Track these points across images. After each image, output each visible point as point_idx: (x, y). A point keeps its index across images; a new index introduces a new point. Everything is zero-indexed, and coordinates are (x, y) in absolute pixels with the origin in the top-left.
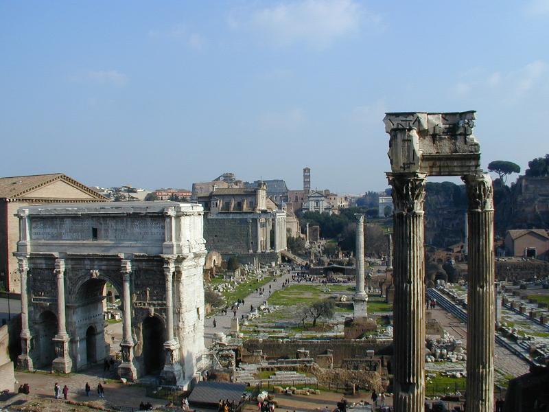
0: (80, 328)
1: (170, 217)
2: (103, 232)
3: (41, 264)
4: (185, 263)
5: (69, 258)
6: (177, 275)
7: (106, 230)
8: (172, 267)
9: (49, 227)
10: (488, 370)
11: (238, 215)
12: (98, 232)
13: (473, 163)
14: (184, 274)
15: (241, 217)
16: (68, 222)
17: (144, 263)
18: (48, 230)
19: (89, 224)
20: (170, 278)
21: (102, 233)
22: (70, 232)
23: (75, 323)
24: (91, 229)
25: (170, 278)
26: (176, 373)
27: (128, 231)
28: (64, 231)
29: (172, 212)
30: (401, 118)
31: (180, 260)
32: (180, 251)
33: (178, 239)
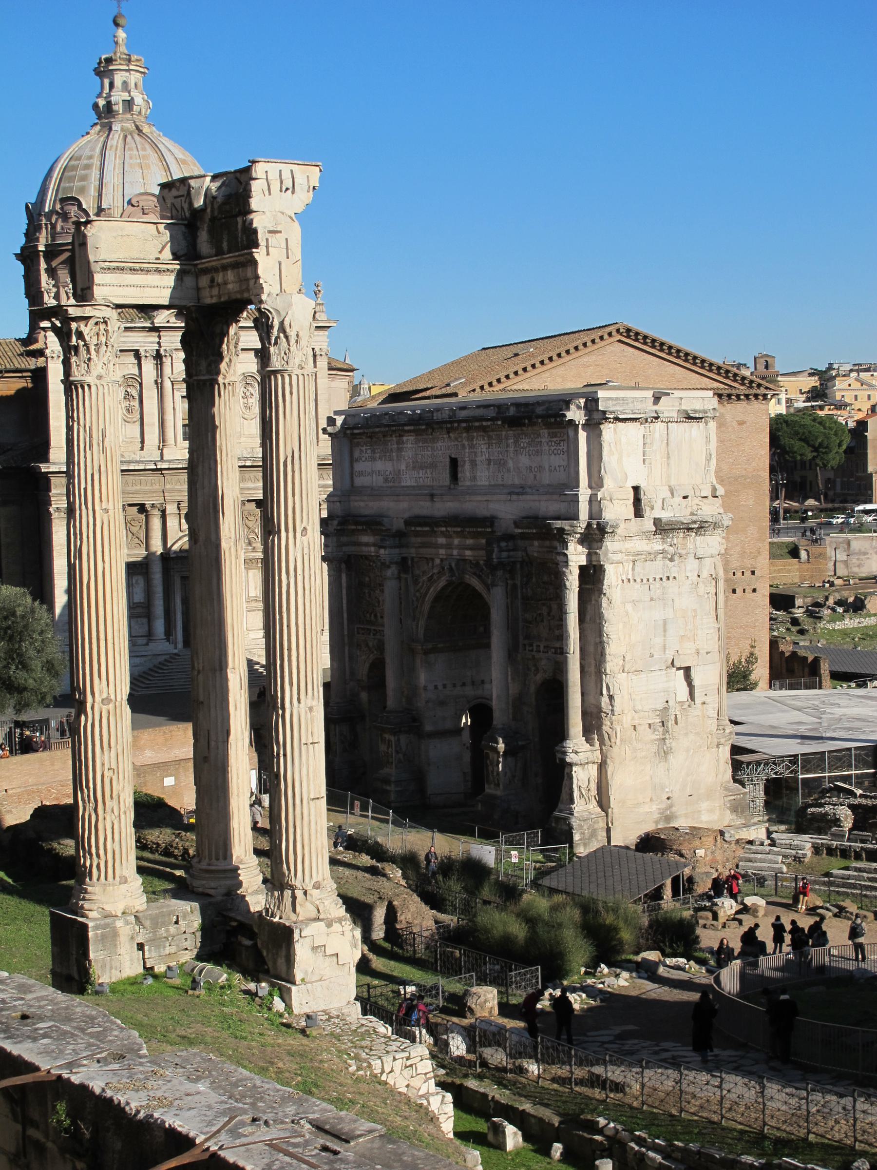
0: (442, 703)
2: (467, 466)
3: (367, 545)
4: (610, 545)
6: (592, 576)
7: (473, 463)
8: (576, 555)
9: (380, 458)
10: (280, 712)
12: (459, 469)
13: (249, 273)
14: (612, 577)
17: (536, 543)
18: (379, 465)
19: (443, 447)
21: (465, 472)
22: (414, 468)
23: (425, 688)
24: (448, 460)
27: (511, 464)
28: (403, 467)
30: (174, 192)
31: (595, 535)
32: (596, 512)
33: (596, 482)
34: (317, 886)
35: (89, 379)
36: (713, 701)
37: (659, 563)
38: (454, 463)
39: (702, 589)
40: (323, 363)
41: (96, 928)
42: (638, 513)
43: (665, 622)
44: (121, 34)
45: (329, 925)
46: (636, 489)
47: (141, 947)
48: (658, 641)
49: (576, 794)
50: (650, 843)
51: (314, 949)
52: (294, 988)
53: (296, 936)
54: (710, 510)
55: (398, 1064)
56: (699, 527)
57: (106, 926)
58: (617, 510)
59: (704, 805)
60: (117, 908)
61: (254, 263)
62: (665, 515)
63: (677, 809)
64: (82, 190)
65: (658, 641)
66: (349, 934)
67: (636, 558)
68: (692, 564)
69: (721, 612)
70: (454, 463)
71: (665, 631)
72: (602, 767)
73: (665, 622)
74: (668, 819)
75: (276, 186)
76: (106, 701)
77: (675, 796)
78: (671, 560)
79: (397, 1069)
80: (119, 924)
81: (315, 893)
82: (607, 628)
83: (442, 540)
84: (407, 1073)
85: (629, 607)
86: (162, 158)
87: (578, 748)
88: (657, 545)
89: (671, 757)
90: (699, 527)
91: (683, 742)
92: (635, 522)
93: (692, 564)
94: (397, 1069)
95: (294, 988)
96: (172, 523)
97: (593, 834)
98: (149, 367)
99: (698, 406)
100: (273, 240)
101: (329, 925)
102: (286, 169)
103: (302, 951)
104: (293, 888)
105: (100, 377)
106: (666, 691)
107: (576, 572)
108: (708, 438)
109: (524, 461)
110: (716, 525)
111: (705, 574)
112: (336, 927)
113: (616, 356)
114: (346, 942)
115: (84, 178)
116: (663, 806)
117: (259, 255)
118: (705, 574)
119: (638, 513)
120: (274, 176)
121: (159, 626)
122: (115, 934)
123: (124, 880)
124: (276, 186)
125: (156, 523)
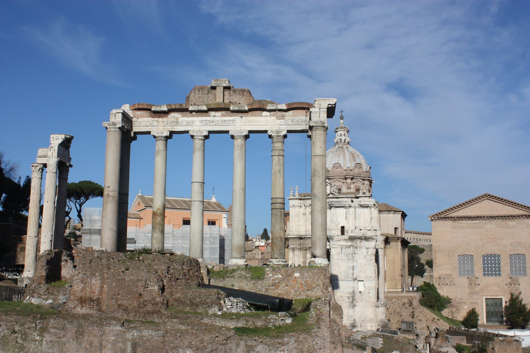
39: (368, 257)
43: (353, 267)
44: (342, 121)
56: (367, 239)
63: (358, 324)
68: (364, 250)
71: (353, 269)
73: (353, 267)
77: (357, 320)
78: (356, 248)
85: (340, 261)
88: (349, 243)
89: (355, 308)
90: (367, 239)
102: (57, 135)
116: (352, 322)
119: (343, 233)
120: (55, 137)
124: (55, 139)
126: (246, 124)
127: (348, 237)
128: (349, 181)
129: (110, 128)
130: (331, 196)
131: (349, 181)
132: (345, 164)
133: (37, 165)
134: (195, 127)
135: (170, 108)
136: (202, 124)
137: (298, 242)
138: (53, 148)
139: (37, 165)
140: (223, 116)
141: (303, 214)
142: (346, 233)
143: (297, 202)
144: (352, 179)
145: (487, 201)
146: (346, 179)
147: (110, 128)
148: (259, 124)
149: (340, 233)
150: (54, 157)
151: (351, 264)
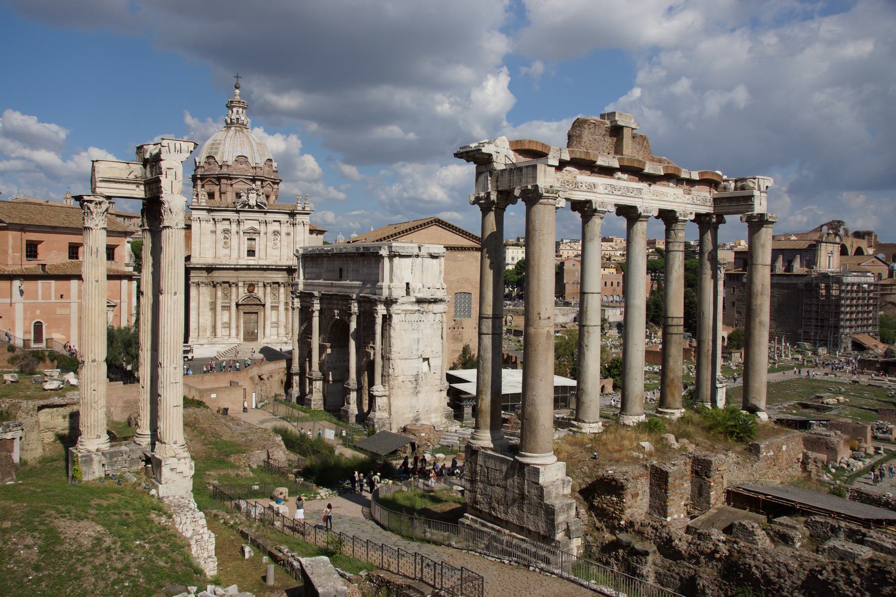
1: (382, 257)
5: (322, 298)
6: (387, 319)
7: (348, 270)
8: (381, 310)
11: (785, 278)
14: (395, 319)
15: (789, 282)
16: (325, 260)
18: (314, 270)
19: (337, 264)
20: (379, 321)
25: (379, 321)
26: (375, 420)
29: (384, 252)
31: (389, 302)
33: (391, 281)
34: (175, 443)
35: (91, 226)
36: (438, 372)
37: (417, 314)
38: (341, 270)
39: (435, 326)
40: (307, 228)
41: (83, 457)
42: (408, 293)
44: (237, 91)
45: (179, 459)
46: (408, 284)
47: (103, 465)
48: (415, 347)
49: (377, 408)
50: (405, 430)
51: (172, 469)
52: (160, 486)
53: (163, 464)
54: (439, 295)
55: (189, 520)
56: (436, 301)
57: (87, 456)
58: (398, 292)
59: (433, 415)
60: (93, 448)
61: (160, 181)
62: (420, 296)
63: (422, 417)
64: (216, 153)
65: (415, 347)
66: (188, 465)
67: (406, 312)
68: (431, 316)
69: (444, 336)
70: (341, 270)
72: (389, 397)
74: (417, 420)
75: (172, 149)
76: (94, 361)
79: (188, 523)
80: (93, 456)
81: (175, 446)
82: (392, 340)
83: (335, 302)
84: (193, 524)
85: (403, 332)
86: (250, 142)
87: (378, 389)
88: (416, 307)
89: (419, 395)
90: (436, 301)
91: (424, 389)
92: (406, 299)
93: (431, 316)
94: (188, 523)
95: (160, 486)
96: (241, 290)
97: (384, 425)
98: (234, 227)
99: (436, 251)
100: (169, 172)
101: (179, 459)
102: (178, 143)
103: (165, 470)
104: (164, 443)
105: (97, 225)
106: (418, 367)
107: (381, 317)
108: (440, 265)
109: (366, 270)
110: (441, 301)
111: (437, 320)
112: (183, 460)
113: (434, 229)
114: (187, 467)
115: (217, 148)
117: (162, 178)
118: (437, 320)
119: (408, 293)
121: (234, 332)
122: (92, 460)
123: (99, 437)
124: (172, 149)
125: (234, 289)
126: (654, 197)
127: (414, 300)
128: (259, 183)
129: (548, 198)
130: (256, 209)
131: (259, 183)
132: (254, 158)
133: (101, 199)
134: (598, 195)
135: (573, 156)
136: (606, 191)
137: (205, 274)
138: (173, 172)
139: (101, 199)
140: (630, 180)
141: (212, 232)
142: (411, 293)
143: (203, 214)
144: (262, 181)
145: (435, 227)
146: (254, 180)
147: (548, 198)
148: (666, 199)
149: (404, 293)
150: (175, 190)
151: (416, 336)
